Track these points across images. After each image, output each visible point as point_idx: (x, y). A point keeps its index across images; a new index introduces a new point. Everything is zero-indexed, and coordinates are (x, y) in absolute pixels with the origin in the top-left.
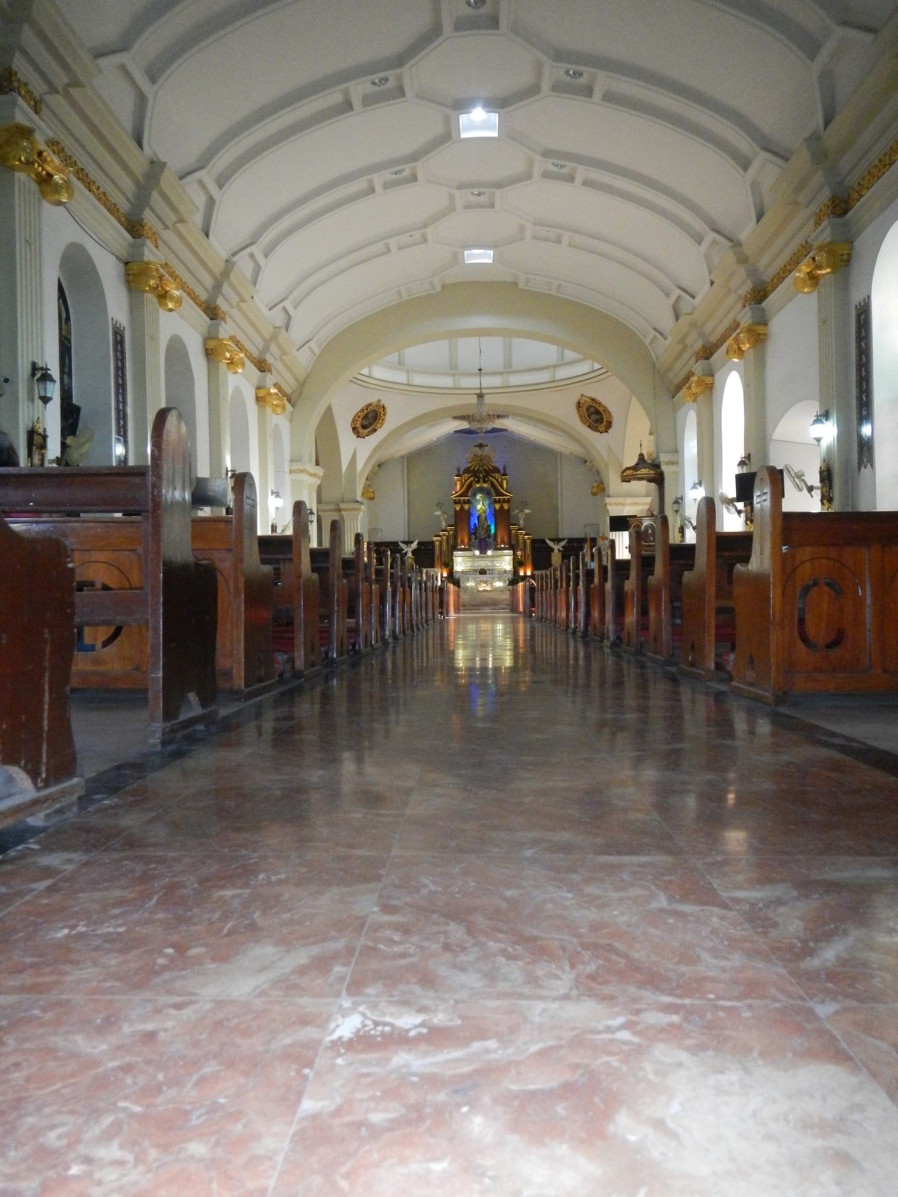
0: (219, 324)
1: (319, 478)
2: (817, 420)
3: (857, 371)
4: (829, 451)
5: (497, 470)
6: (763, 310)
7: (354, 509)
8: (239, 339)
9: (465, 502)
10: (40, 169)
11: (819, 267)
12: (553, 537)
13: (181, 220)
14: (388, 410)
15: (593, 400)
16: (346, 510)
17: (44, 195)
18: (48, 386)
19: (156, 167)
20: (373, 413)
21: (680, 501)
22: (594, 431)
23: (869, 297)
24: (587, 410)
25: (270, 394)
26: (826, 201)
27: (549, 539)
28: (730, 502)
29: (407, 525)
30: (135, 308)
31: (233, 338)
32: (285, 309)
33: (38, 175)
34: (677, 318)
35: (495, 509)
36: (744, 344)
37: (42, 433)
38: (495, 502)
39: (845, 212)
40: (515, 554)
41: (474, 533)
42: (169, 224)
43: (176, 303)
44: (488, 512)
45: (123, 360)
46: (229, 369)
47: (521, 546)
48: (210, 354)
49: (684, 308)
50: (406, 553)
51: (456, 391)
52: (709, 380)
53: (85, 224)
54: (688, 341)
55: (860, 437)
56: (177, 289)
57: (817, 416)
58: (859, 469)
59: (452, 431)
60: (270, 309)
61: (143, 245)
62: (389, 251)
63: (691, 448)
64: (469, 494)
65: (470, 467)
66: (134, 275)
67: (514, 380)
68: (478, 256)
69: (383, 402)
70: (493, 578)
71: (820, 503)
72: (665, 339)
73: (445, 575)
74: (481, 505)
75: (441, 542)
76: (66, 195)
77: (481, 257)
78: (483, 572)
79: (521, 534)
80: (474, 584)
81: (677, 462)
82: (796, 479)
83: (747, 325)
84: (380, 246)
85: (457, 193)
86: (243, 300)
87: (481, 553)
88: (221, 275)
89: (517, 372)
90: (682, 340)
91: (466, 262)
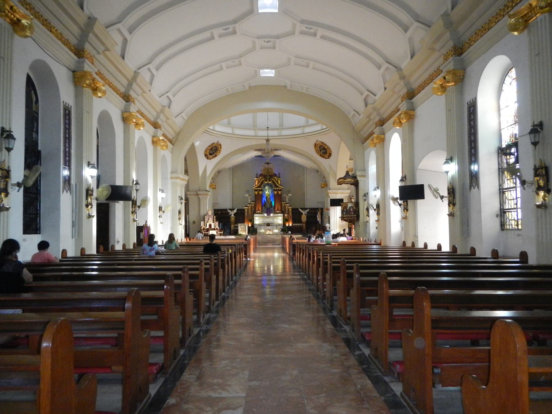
0: (131, 104)
1: (186, 181)
2: (447, 162)
3: (468, 137)
4: (453, 178)
5: (275, 175)
6: (413, 103)
7: (205, 194)
8: (143, 112)
9: (260, 190)
10: (12, 16)
11: (448, 82)
12: (302, 207)
13: (108, 50)
14: (222, 146)
15: (322, 143)
16: (200, 194)
17: (15, 31)
18: (10, 141)
19: (91, 20)
20: (216, 148)
21: (367, 195)
22: (323, 157)
23: (476, 98)
24: (319, 147)
25: (159, 140)
26: (450, 48)
27: (300, 209)
28: (395, 199)
29: (231, 201)
30: (78, 96)
31: (139, 112)
32: (168, 97)
33: (11, 20)
34: (366, 106)
35: (274, 193)
36: (403, 119)
37: (7, 169)
38: (275, 190)
39: (461, 54)
40: (284, 216)
41: (264, 205)
42: (101, 52)
43: (102, 93)
44: (271, 195)
45: (70, 124)
46: (136, 127)
47: (287, 212)
48: (125, 120)
49: (370, 101)
50: (231, 214)
51: (256, 138)
52: (383, 136)
53: (45, 48)
54: (372, 117)
55: (471, 172)
56: (104, 85)
57: (446, 159)
58: (470, 189)
59: (254, 156)
60: (160, 97)
61: (84, 61)
62: (222, 69)
63: (372, 169)
64: (262, 187)
65: (263, 174)
66: (78, 78)
67: (285, 132)
68: (267, 73)
69: (220, 142)
70: (273, 228)
71: (447, 205)
72: (360, 115)
73: (250, 225)
74: (267, 192)
75: (248, 209)
76: (29, 31)
77: (269, 73)
78: (268, 225)
79: (287, 206)
80: (264, 231)
81: (365, 176)
82: (434, 192)
83: (404, 110)
84: (218, 66)
85: (257, 41)
86: (144, 92)
87: (267, 215)
88: (132, 79)
89: (285, 129)
90: (369, 117)
91: (261, 76)
